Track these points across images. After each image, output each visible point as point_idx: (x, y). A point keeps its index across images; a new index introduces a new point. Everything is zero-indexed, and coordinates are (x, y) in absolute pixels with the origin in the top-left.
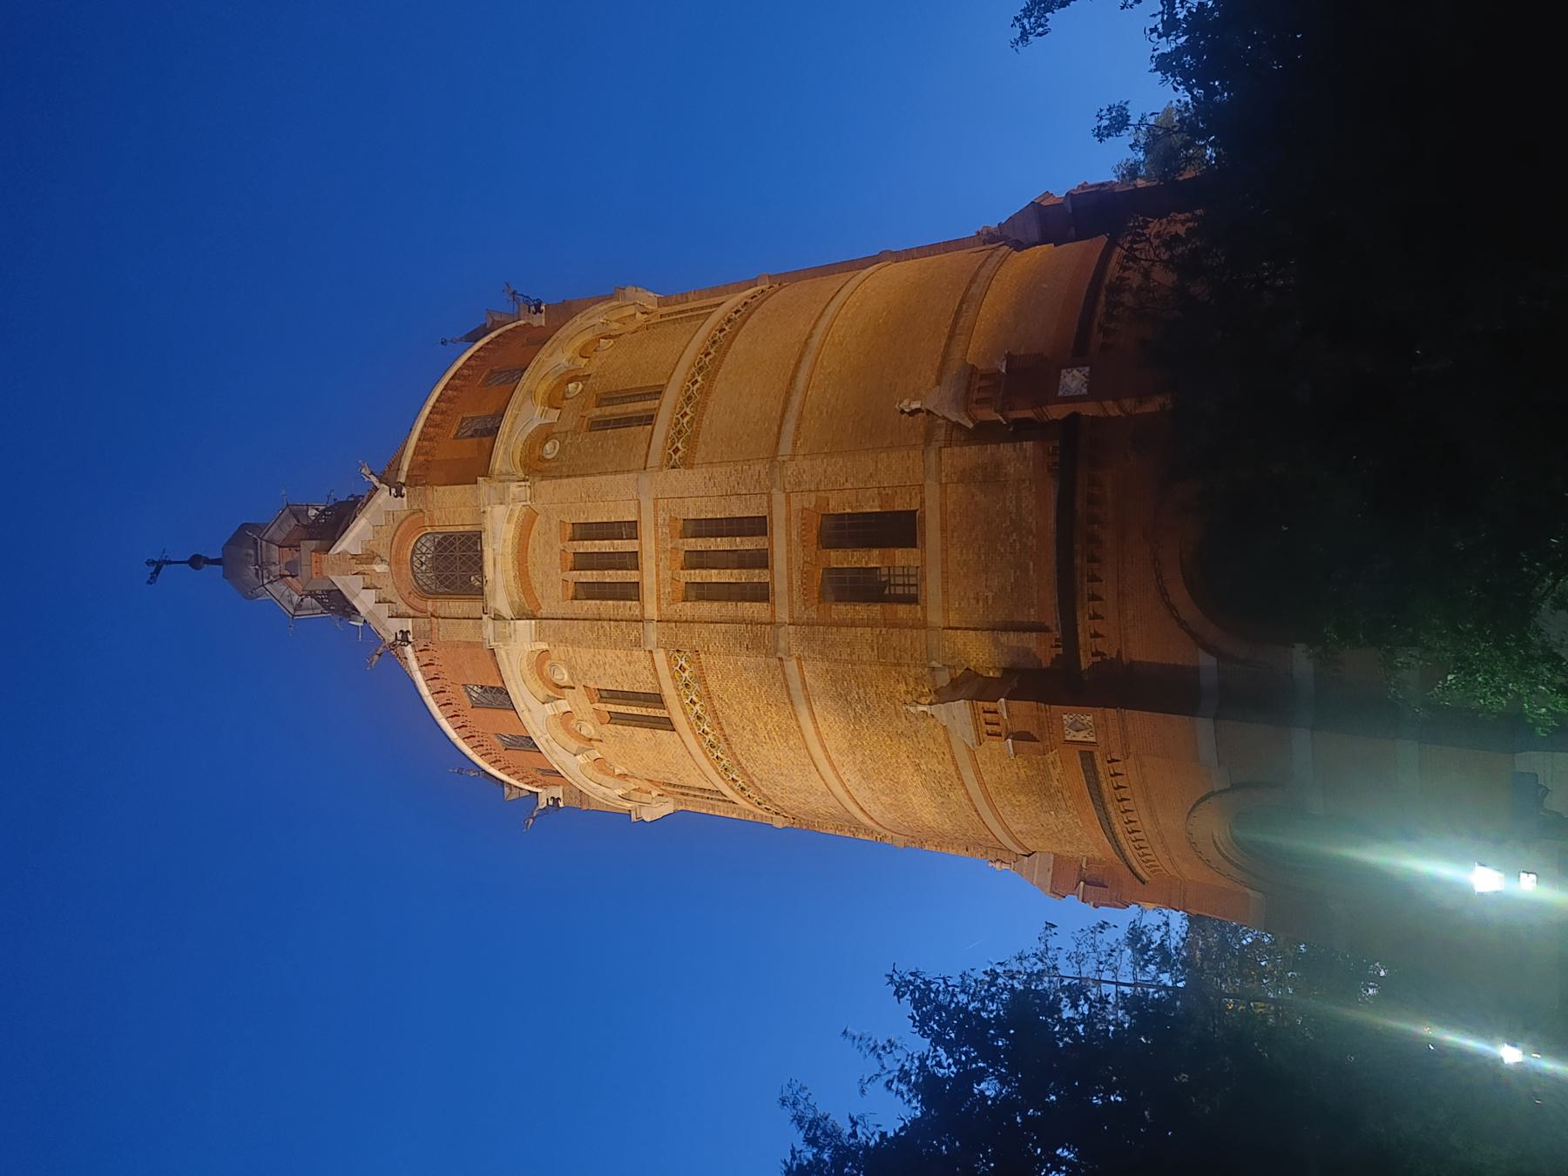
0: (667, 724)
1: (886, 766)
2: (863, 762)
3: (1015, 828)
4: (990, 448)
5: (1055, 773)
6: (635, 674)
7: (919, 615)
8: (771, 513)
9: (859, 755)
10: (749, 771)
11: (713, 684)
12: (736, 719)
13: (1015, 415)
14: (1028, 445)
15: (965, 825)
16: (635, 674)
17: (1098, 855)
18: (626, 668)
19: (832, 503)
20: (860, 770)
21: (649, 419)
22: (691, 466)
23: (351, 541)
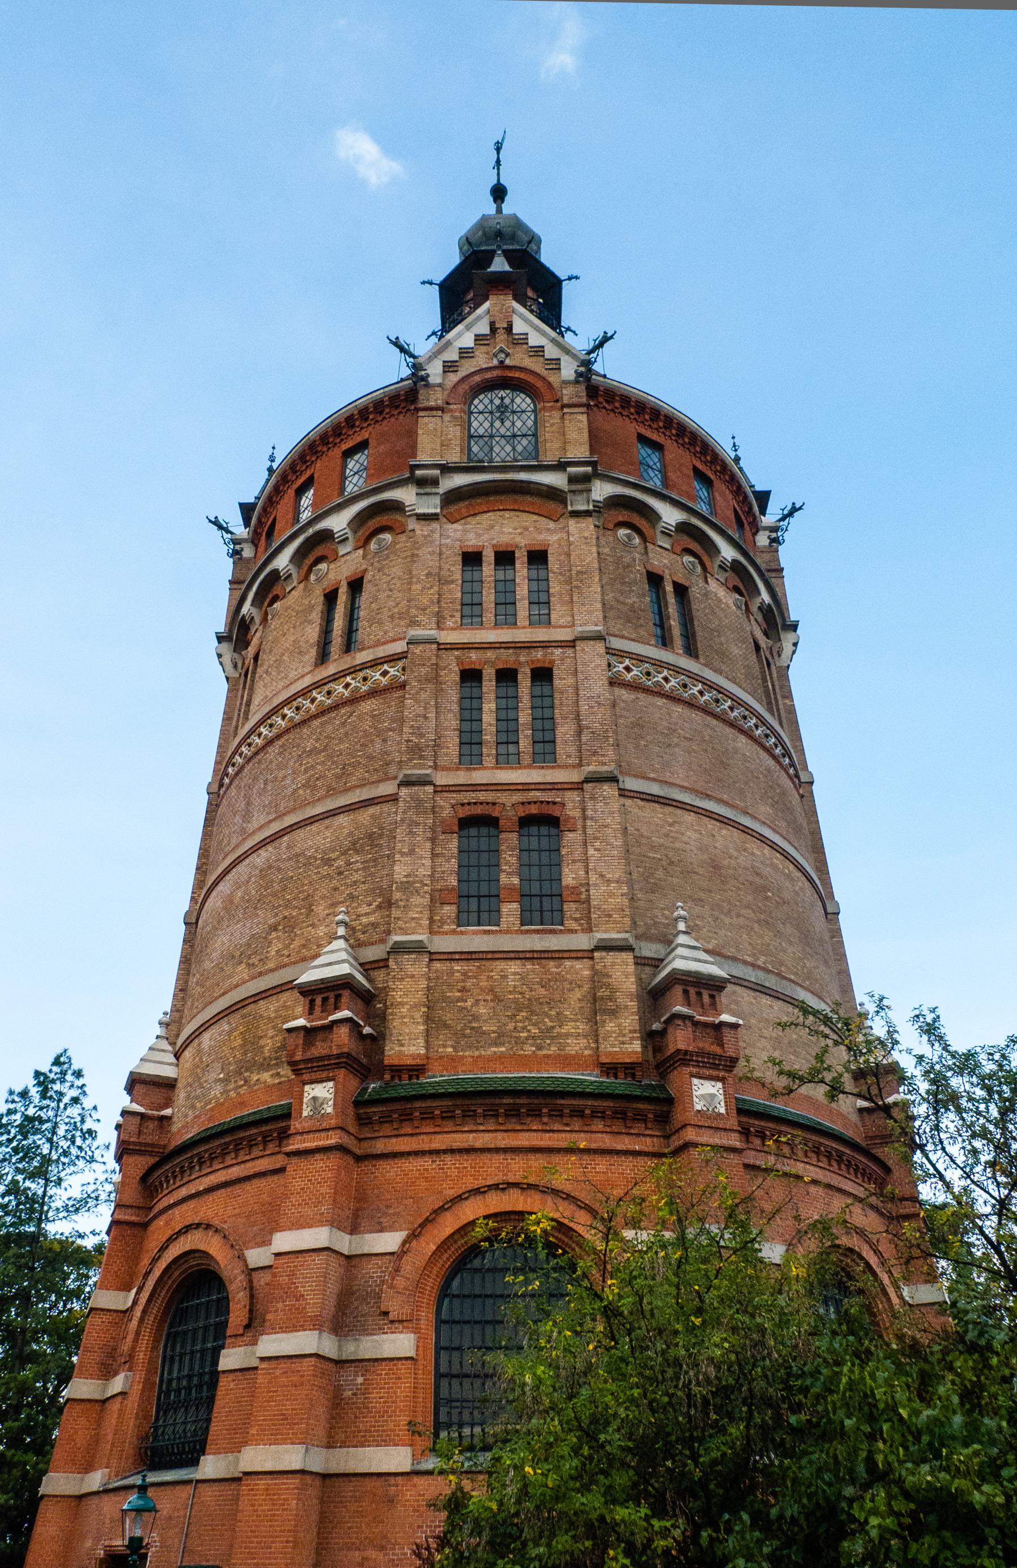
0: (323, 657)
1: (275, 895)
2: (279, 869)
3: (206, 1039)
4: (633, 1005)
5: (266, 1076)
6: (380, 623)
7: (446, 927)
8: (559, 767)
9: (288, 864)
10: (270, 749)
11: (366, 706)
12: (329, 728)
13: (662, 1020)
14: (637, 1046)
15: (208, 984)
16: (380, 623)
17: (174, 1128)
18: (386, 613)
19: (571, 835)
20: (270, 867)
21: (665, 642)
22: (612, 683)
23: (525, 322)
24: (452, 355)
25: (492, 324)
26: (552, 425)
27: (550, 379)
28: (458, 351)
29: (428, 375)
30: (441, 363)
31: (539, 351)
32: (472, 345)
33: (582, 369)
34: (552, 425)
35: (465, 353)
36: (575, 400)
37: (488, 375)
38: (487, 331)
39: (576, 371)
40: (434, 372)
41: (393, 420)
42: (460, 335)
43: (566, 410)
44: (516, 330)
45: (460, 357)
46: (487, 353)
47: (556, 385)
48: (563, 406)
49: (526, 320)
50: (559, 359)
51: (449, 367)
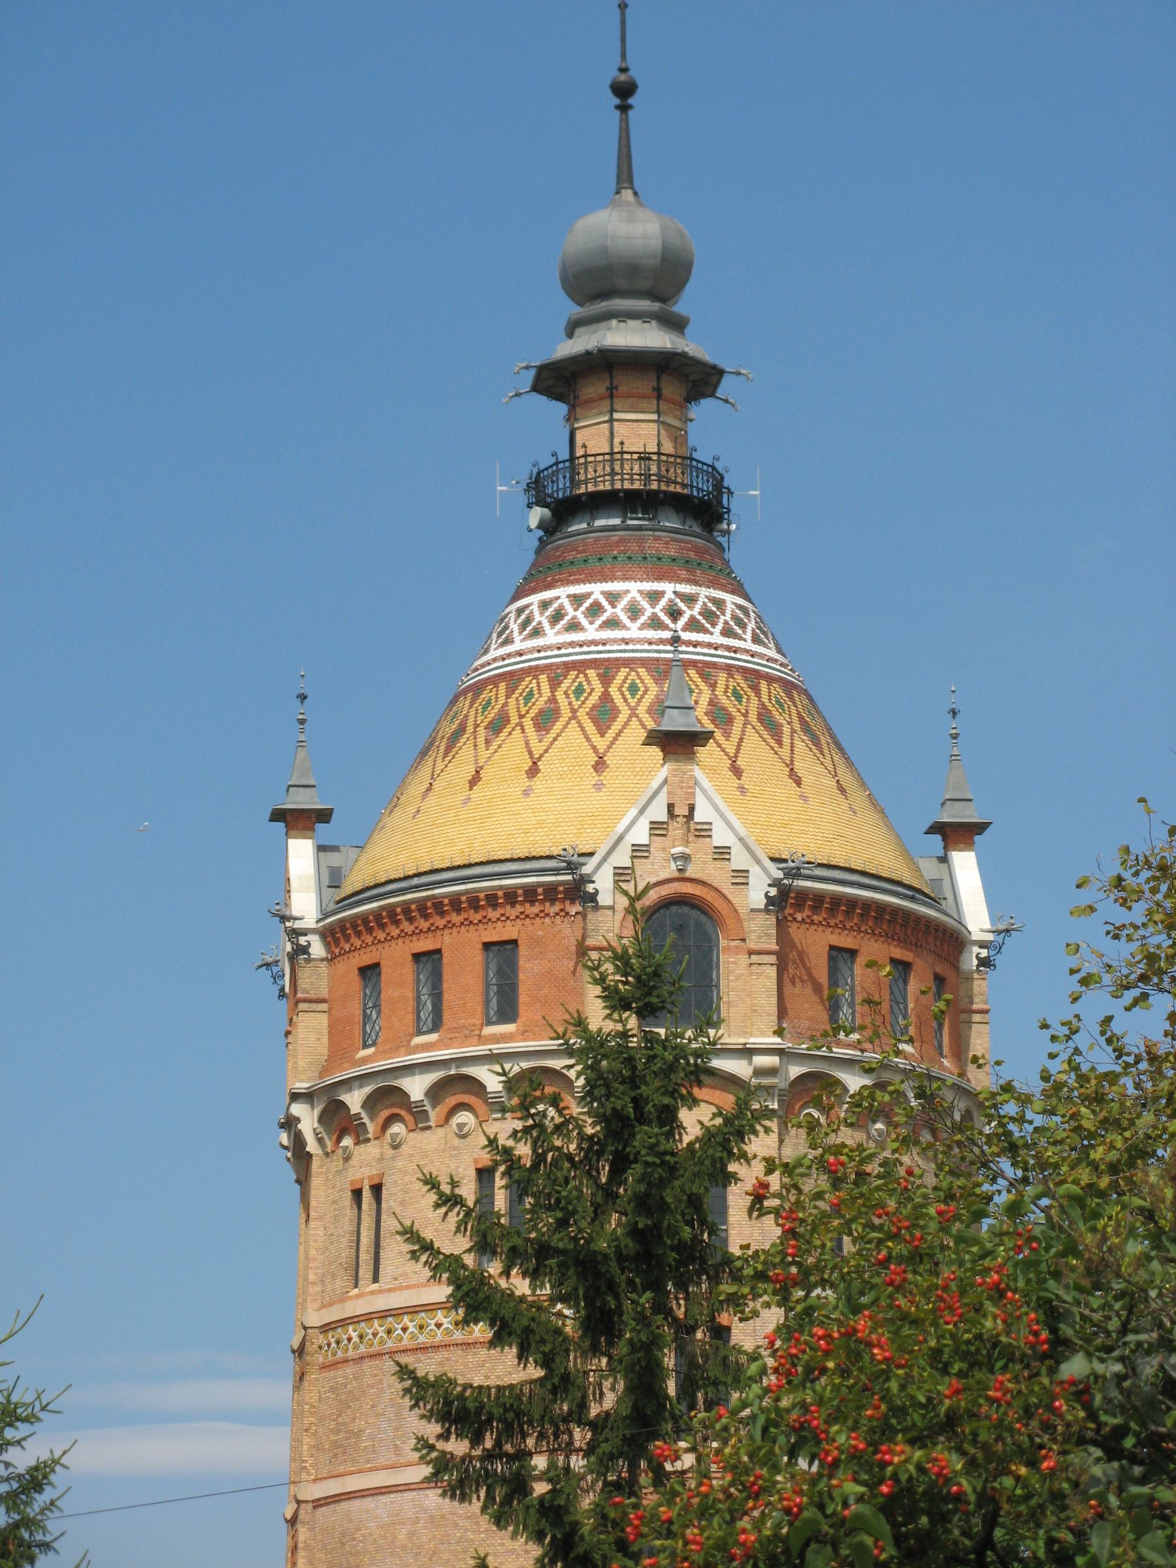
24: (622, 858)
25: (671, 807)
26: (738, 978)
27: (734, 900)
28: (630, 848)
29: (597, 892)
30: (611, 871)
31: (723, 853)
32: (647, 842)
33: (773, 892)
34: (738, 978)
35: (639, 851)
36: (765, 947)
37: (665, 891)
38: (663, 816)
39: (766, 895)
40: (603, 884)
41: (547, 920)
42: (633, 823)
43: (754, 958)
44: (698, 817)
45: (633, 857)
46: (664, 850)
47: (741, 910)
48: (751, 953)
49: (709, 799)
50: (747, 871)
51: (621, 874)
